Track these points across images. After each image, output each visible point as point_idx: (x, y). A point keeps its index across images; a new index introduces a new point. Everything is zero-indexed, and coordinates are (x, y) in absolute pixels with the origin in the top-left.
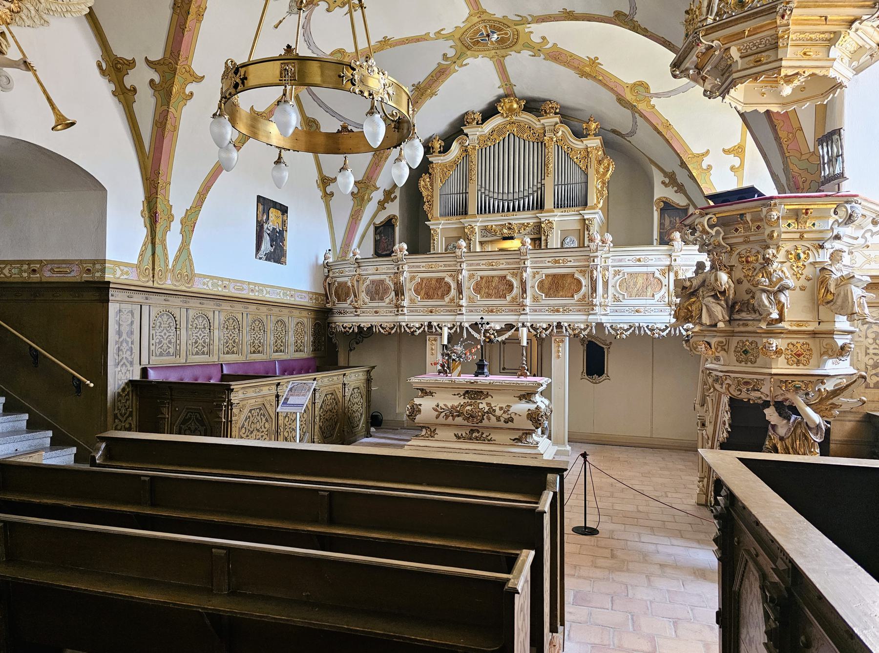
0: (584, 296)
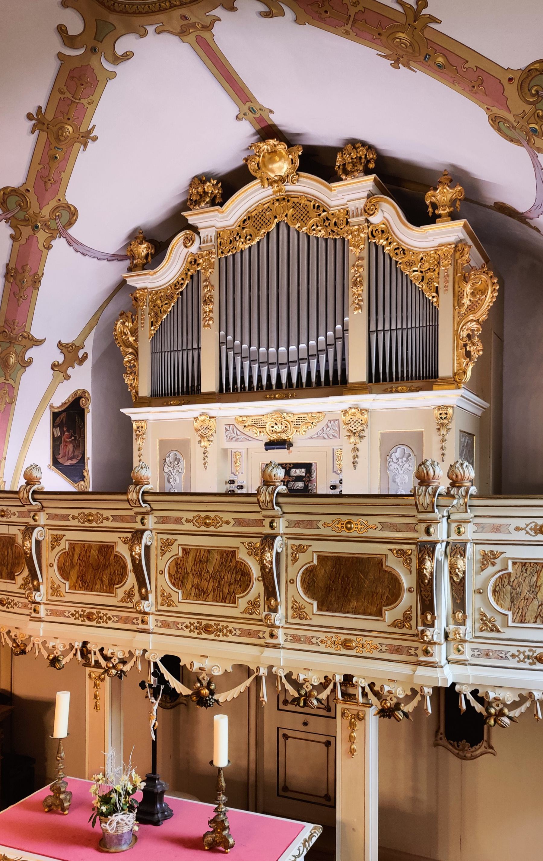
0: (407, 618)
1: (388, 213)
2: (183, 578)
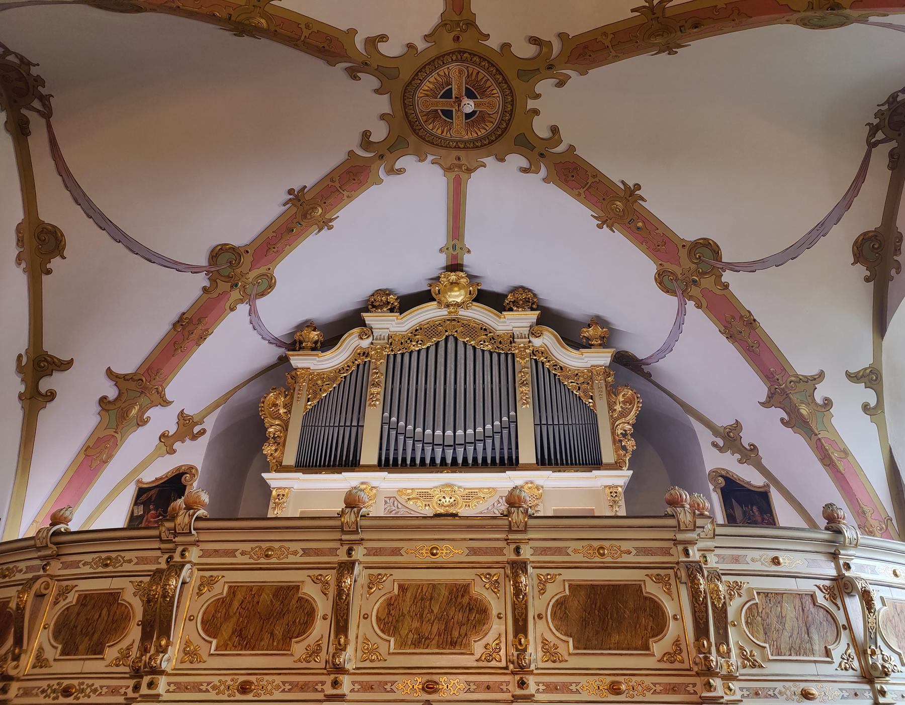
1: (548, 340)
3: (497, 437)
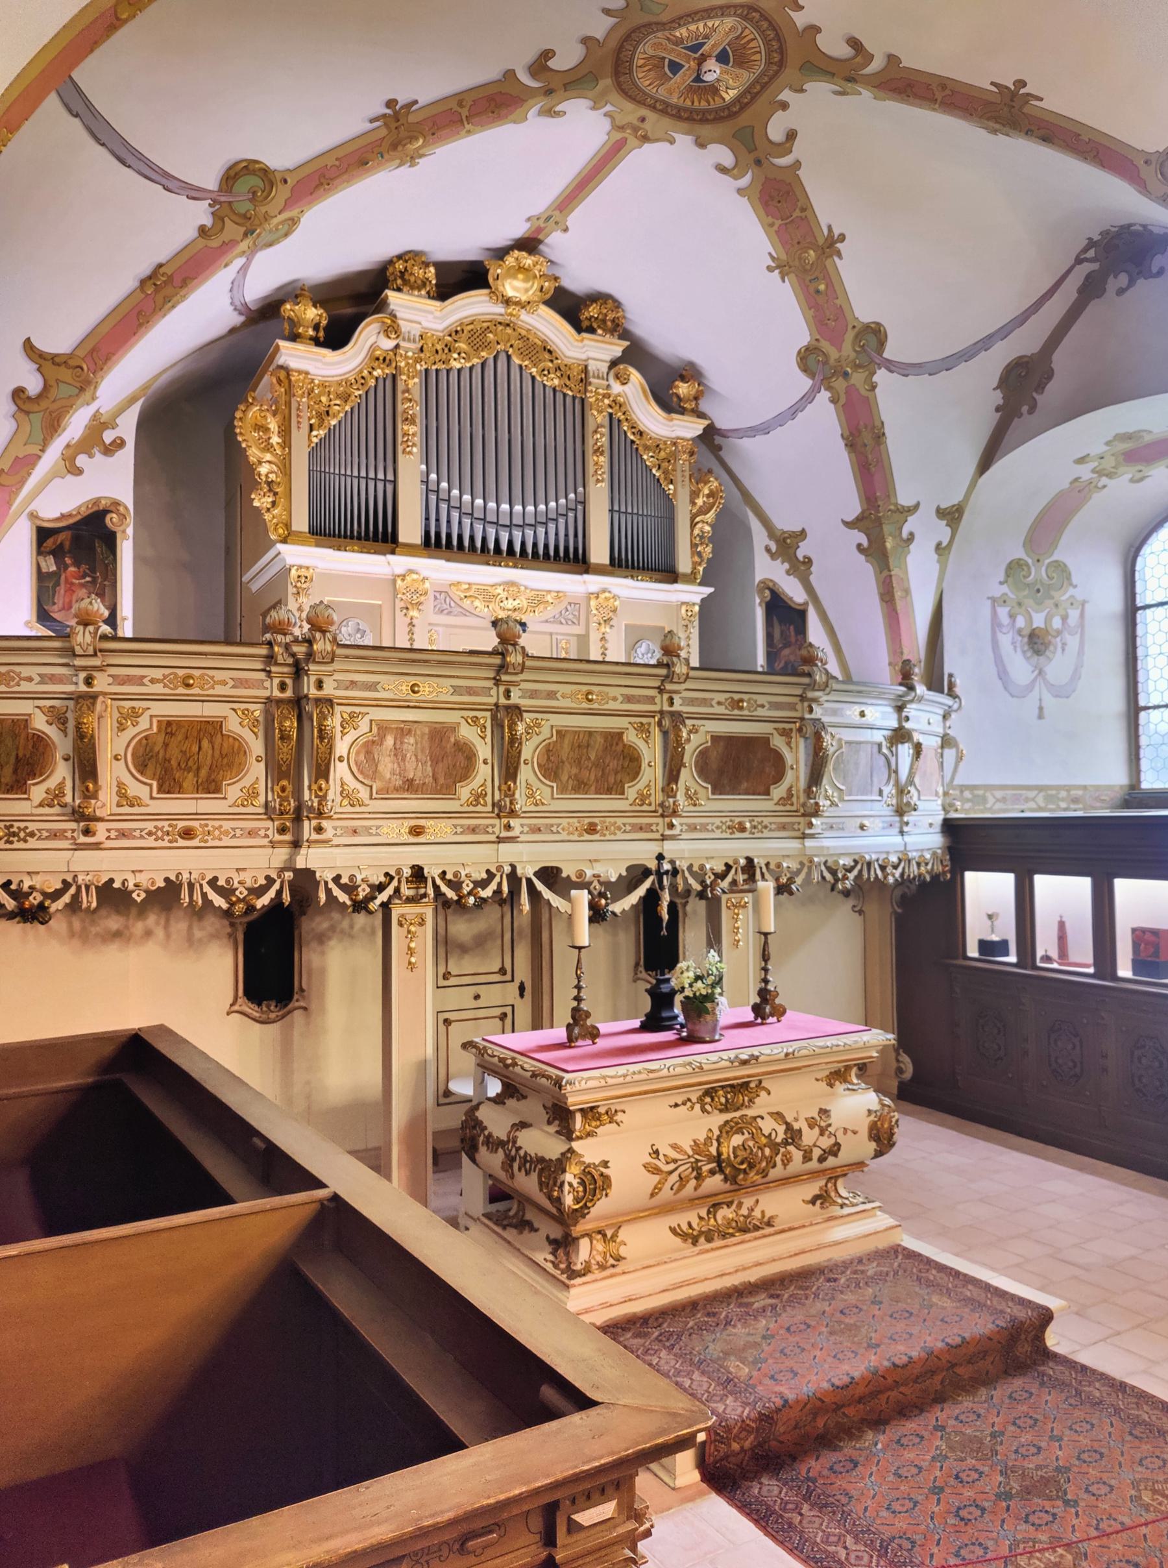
2: (557, 767)
3: (562, 521)
